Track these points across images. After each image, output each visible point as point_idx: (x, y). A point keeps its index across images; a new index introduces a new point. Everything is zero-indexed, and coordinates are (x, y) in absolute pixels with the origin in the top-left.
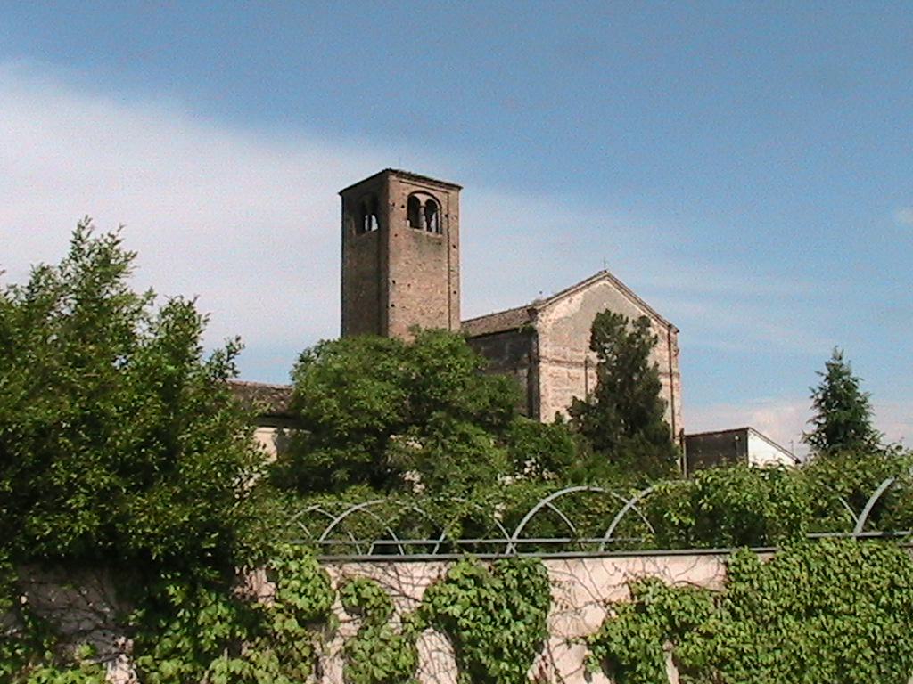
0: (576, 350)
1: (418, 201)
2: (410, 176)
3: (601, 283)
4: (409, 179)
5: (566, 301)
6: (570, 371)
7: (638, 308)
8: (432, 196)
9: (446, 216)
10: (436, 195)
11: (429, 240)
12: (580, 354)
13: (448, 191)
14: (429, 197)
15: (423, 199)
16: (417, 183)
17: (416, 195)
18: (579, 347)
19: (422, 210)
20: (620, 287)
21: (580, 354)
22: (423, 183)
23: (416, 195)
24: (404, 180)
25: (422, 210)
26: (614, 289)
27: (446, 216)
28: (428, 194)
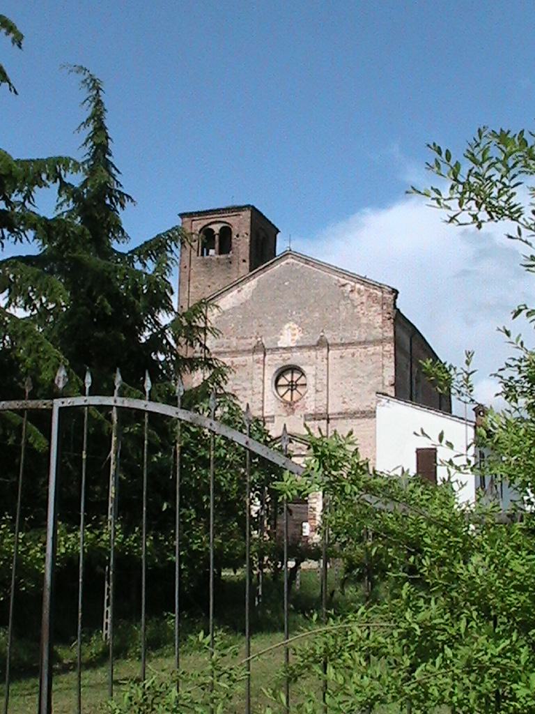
0: (243, 338)
1: (212, 231)
2: (199, 214)
3: (283, 263)
4: (199, 216)
5: (235, 292)
6: (234, 359)
7: (337, 278)
8: (225, 223)
9: (238, 236)
10: (227, 221)
11: (219, 262)
12: (249, 341)
13: (240, 213)
14: (222, 225)
15: (216, 228)
16: (208, 217)
17: (210, 227)
18: (248, 334)
19: (217, 237)
20: (307, 261)
21: (249, 341)
22: (213, 214)
23: (210, 227)
24: (195, 218)
25: (217, 237)
26: (302, 264)
27: (238, 236)
28: (220, 222)
